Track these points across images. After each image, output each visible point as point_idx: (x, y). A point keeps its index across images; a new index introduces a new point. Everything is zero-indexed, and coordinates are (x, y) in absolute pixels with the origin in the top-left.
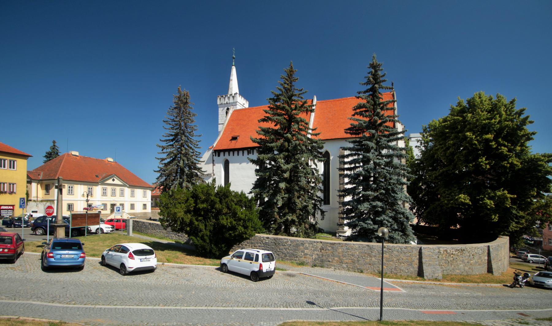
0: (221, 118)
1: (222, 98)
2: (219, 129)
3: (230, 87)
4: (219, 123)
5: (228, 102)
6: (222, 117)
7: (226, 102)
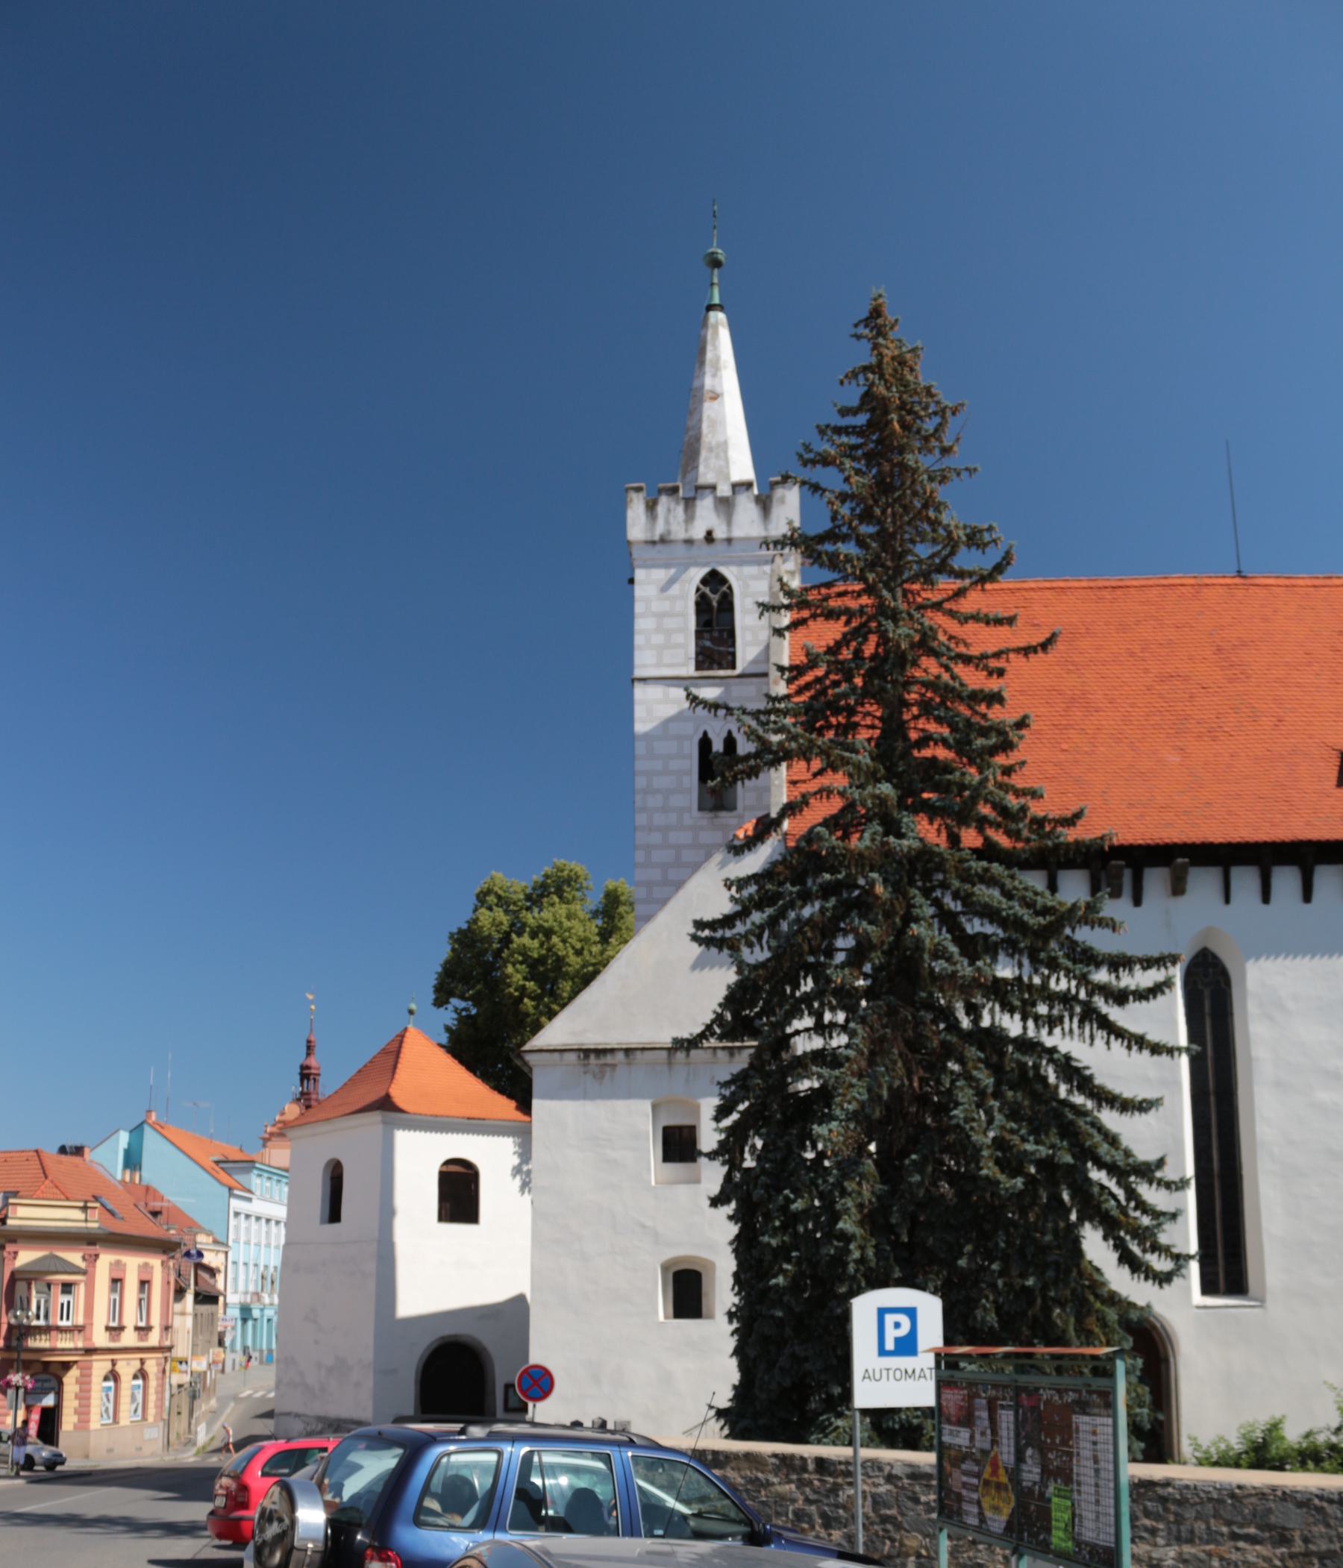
0: (658, 639)
1: (664, 501)
2: (639, 711)
3: (708, 437)
4: (638, 673)
5: (720, 533)
6: (658, 630)
7: (698, 533)
